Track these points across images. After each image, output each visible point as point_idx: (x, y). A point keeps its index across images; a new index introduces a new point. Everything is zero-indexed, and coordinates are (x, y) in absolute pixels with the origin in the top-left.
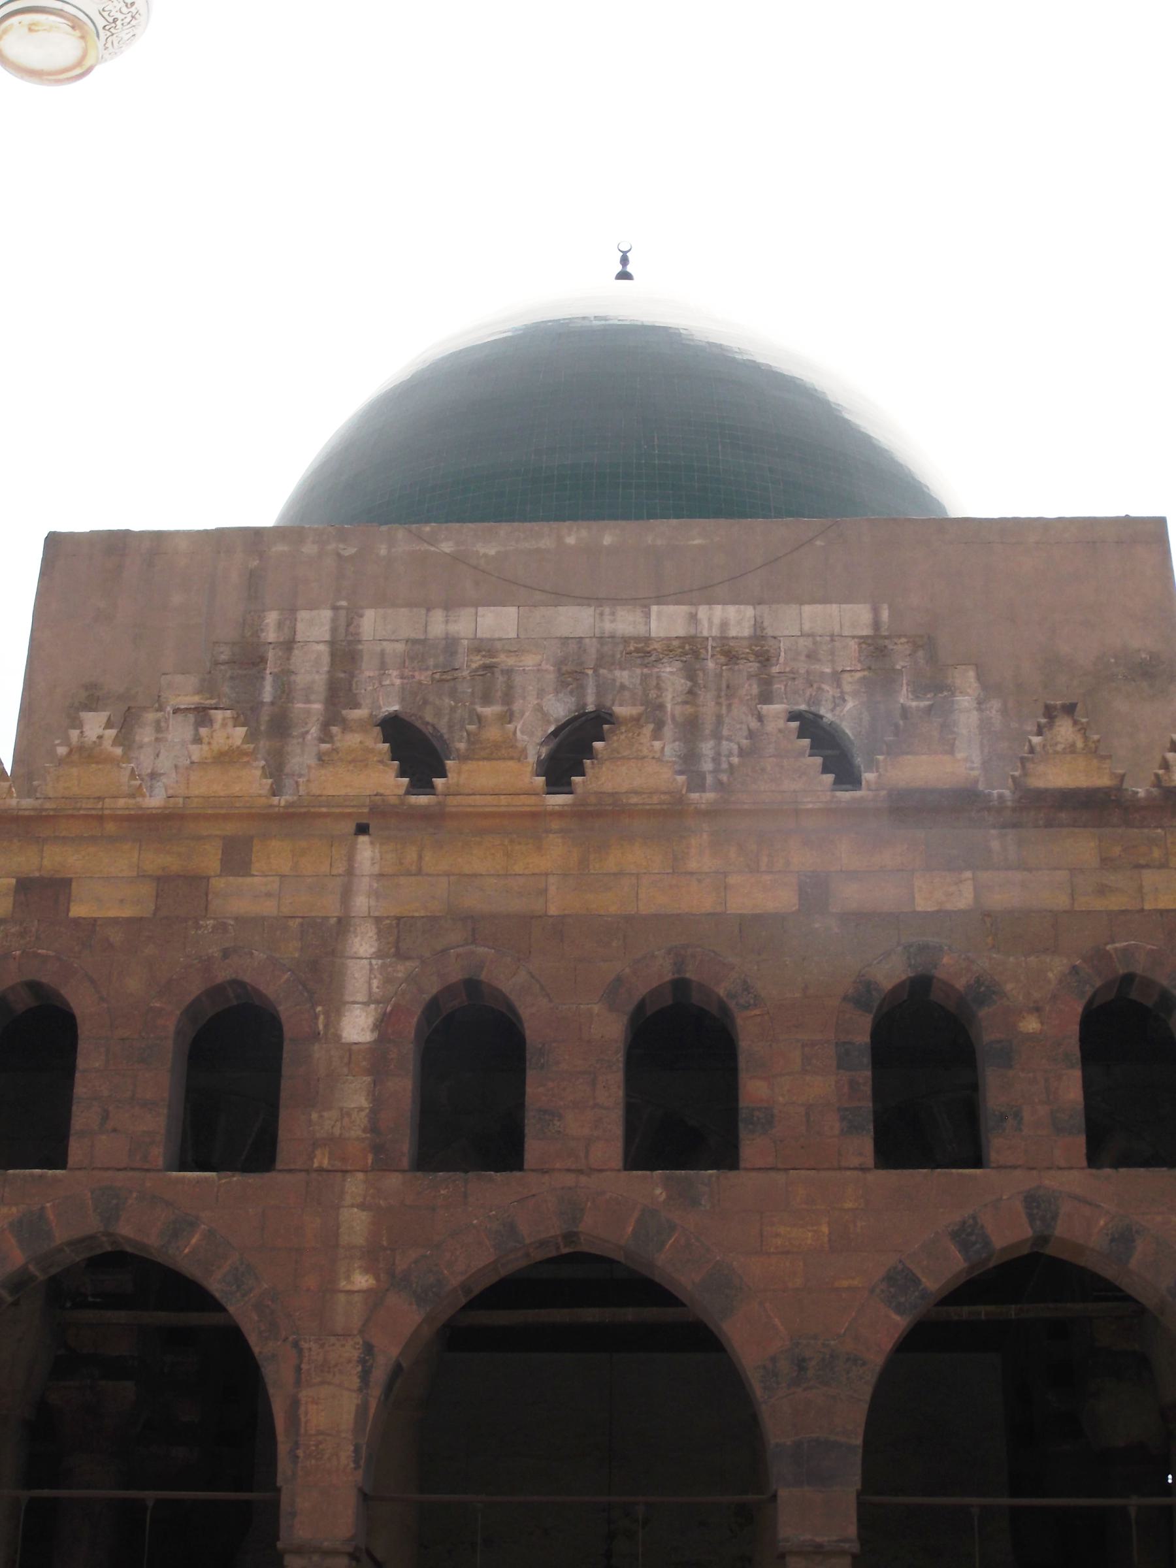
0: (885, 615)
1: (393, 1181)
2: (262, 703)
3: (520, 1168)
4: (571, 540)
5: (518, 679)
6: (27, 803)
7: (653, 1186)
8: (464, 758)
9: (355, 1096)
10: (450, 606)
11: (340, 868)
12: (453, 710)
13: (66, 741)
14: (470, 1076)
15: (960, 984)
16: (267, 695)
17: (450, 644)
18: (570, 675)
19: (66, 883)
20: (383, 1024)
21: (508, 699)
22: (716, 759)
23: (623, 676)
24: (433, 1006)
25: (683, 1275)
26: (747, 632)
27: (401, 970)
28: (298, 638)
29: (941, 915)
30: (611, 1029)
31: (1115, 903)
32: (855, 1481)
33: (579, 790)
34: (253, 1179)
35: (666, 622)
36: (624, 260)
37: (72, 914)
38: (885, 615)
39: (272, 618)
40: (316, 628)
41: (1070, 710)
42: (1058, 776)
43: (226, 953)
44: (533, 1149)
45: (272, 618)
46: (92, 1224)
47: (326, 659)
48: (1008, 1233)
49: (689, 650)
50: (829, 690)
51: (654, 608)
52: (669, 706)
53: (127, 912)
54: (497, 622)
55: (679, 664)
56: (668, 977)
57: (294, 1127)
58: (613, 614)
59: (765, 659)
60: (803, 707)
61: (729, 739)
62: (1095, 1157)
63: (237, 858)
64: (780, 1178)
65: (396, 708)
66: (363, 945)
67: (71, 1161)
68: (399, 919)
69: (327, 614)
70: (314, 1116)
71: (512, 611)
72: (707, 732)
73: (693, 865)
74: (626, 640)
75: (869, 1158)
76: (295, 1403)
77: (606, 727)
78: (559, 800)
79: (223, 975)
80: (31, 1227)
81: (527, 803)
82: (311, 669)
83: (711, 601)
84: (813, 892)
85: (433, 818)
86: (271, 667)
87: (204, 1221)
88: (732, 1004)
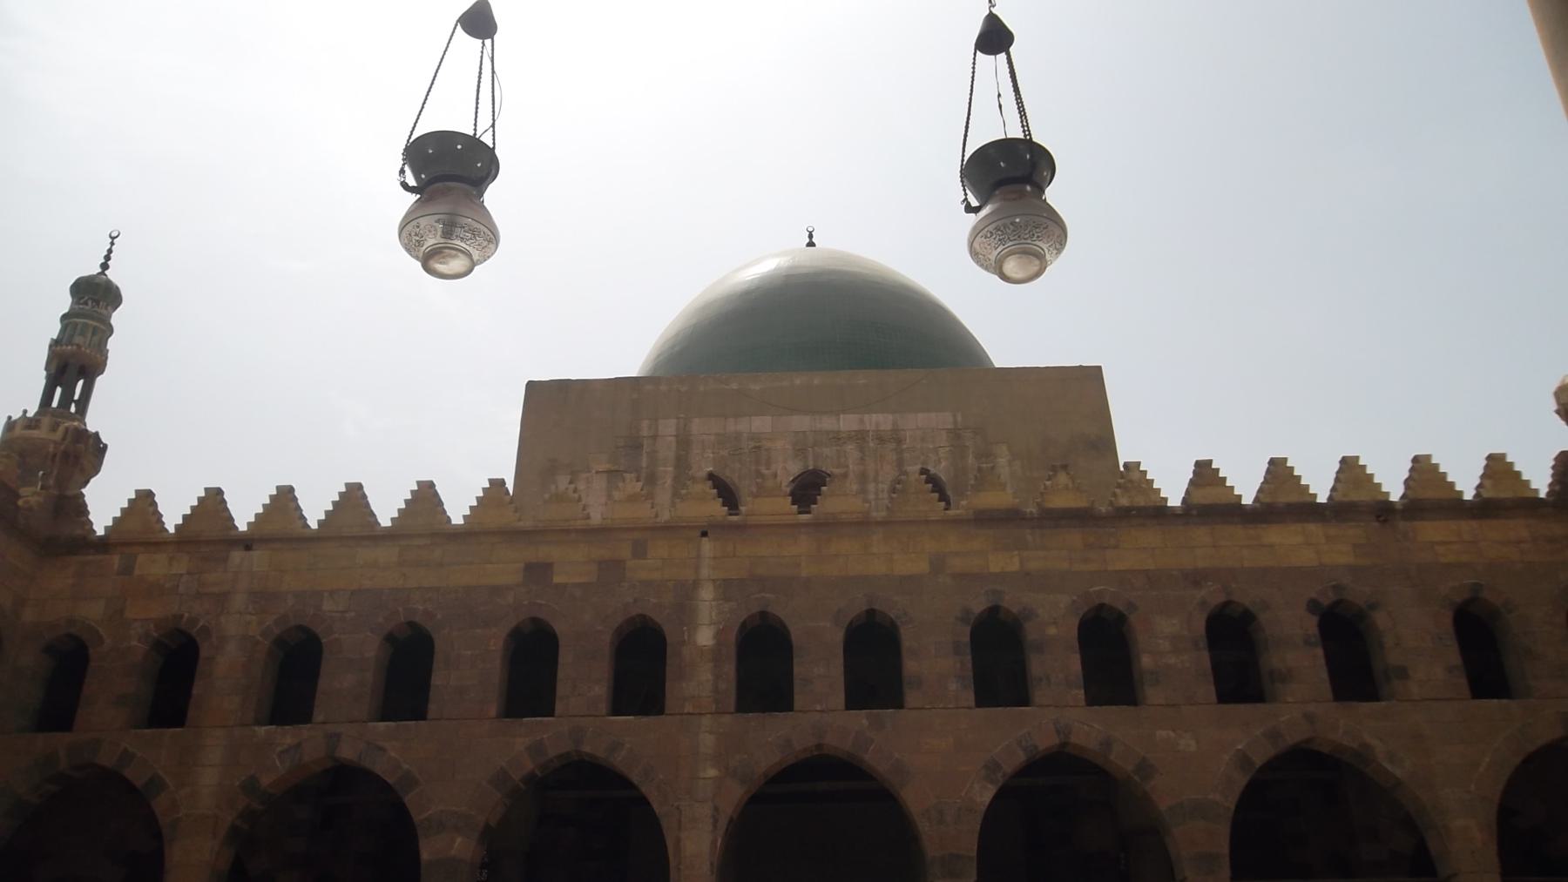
0: (959, 418)
1: (727, 719)
4: (798, 382)
7: (861, 718)
8: (756, 496)
16: (644, 462)
20: (719, 635)
22: (876, 494)
23: (826, 451)
24: (744, 624)
26: (889, 427)
34: (652, 718)
35: (848, 423)
36: (811, 236)
38: (959, 418)
39: (645, 424)
40: (668, 428)
41: (1065, 467)
42: (1060, 502)
43: (636, 601)
44: (799, 701)
45: (645, 424)
48: (1046, 741)
49: (860, 436)
59: (899, 441)
62: (1092, 701)
63: (640, 551)
66: (707, 594)
67: (557, 712)
69: (674, 421)
71: (769, 418)
74: (828, 432)
75: (973, 704)
76: (678, 841)
82: (667, 449)
85: (740, 528)
86: (646, 449)
87: (628, 742)
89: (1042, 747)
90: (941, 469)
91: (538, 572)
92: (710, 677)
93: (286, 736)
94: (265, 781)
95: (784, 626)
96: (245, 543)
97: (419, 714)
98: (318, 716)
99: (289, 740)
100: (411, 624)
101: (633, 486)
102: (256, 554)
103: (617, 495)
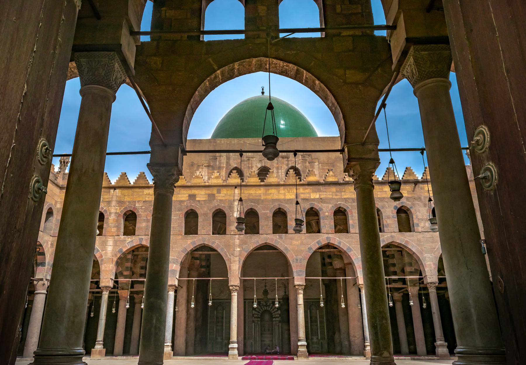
3: (258, 233)
11: (233, 192)
15: (317, 208)
16: (218, 163)
19: (195, 195)
21: (252, 164)
25: (282, 248)
29: (314, 200)
30: (271, 215)
31: (338, 197)
41: (332, 170)
42: (330, 179)
46: (202, 243)
53: (204, 199)
63: (219, 192)
73: (281, 192)
76: (230, 266)
78: (262, 183)
80: (193, 243)
81: (258, 184)
85: (246, 186)
87: (216, 242)
89: (323, 244)
91: (192, 197)
93: (129, 239)
94: (124, 250)
96: (115, 188)
98: (136, 233)
99: (129, 240)
101: (216, 174)
102: (117, 191)
103: (212, 177)
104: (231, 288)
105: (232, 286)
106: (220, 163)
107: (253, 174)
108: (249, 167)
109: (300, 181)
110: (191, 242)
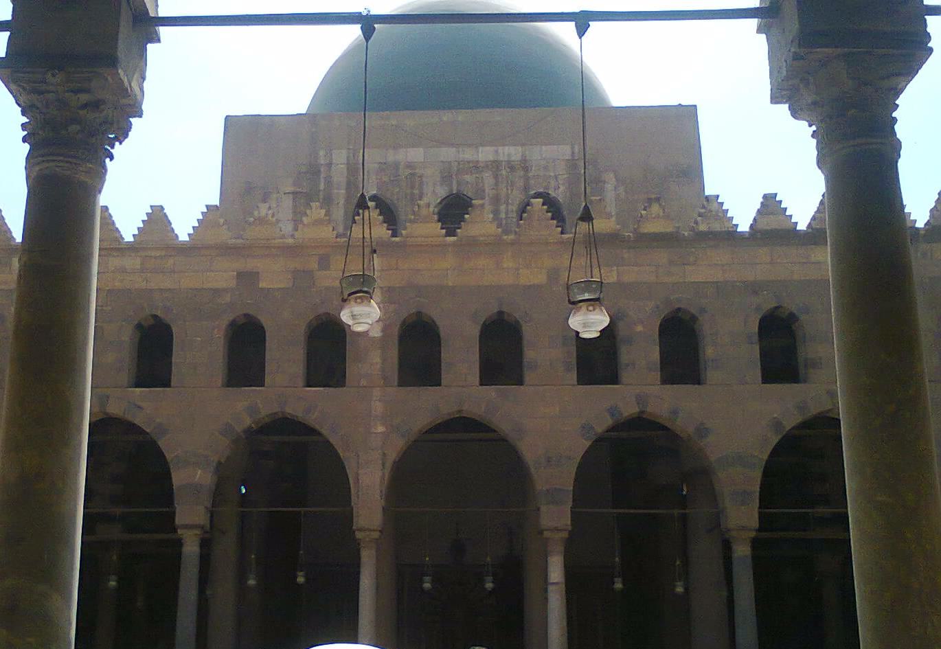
2: (319, 191)
5: (424, 179)
6: (240, 241)
7: (491, 392)
9: (376, 358)
10: (396, 147)
12: (399, 192)
13: (251, 214)
14: (418, 348)
16: (322, 186)
17: (396, 166)
18: (446, 177)
22: (507, 213)
23: (468, 178)
24: (404, 321)
25: (505, 427)
27: (392, 307)
28: (334, 161)
30: (473, 331)
32: (570, 504)
33: (459, 235)
35: (485, 154)
37: (260, 286)
39: (322, 153)
40: (340, 158)
44: (445, 378)
46: (276, 408)
47: (345, 171)
48: (629, 410)
49: (495, 166)
50: (553, 183)
51: (480, 149)
52: (487, 191)
54: (416, 155)
55: (491, 173)
56: (496, 311)
57: (352, 370)
58: (463, 151)
59: (526, 169)
60: (542, 190)
61: (512, 205)
63: (324, 262)
64: (541, 388)
65: (375, 192)
68: (389, 287)
70: (360, 366)
72: (503, 201)
73: (505, 266)
74: (469, 162)
75: (576, 383)
77: (470, 209)
79: (322, 311)
82: (339, 174)
83: (504, 145)
84: (553, 274)
86: (322, 176)
87: (318, 407)
88: (522, 322)
89: (626, 414)
90: (560, 193)
91: (247, 278)
92: (378, 360)
95: (433, 321)
97: (166, 383)
100: (155, 317)
101: (316, 211)
103: (305, 220)
104: (359, 535)
105: (360, 530)
106: (329, 182)
107: (424, 212)
108: (412, 194)
109: (562, 233)
110: (245, 407)
